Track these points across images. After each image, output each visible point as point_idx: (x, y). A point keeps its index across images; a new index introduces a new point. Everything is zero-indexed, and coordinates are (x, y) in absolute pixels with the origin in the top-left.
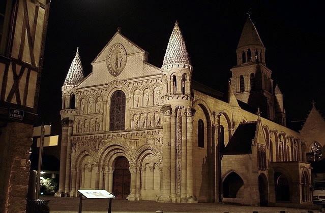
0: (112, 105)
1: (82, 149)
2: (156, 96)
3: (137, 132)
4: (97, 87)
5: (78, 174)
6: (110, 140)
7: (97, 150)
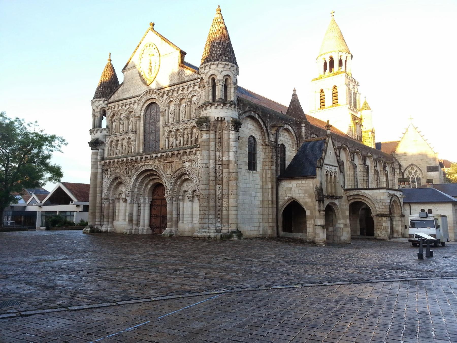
1: (114, 176)
2: (193, 106)
3: (172, 153)
4: (128, 100)
5: (111, 205)
6: (143, 164)
7: (129, 177)
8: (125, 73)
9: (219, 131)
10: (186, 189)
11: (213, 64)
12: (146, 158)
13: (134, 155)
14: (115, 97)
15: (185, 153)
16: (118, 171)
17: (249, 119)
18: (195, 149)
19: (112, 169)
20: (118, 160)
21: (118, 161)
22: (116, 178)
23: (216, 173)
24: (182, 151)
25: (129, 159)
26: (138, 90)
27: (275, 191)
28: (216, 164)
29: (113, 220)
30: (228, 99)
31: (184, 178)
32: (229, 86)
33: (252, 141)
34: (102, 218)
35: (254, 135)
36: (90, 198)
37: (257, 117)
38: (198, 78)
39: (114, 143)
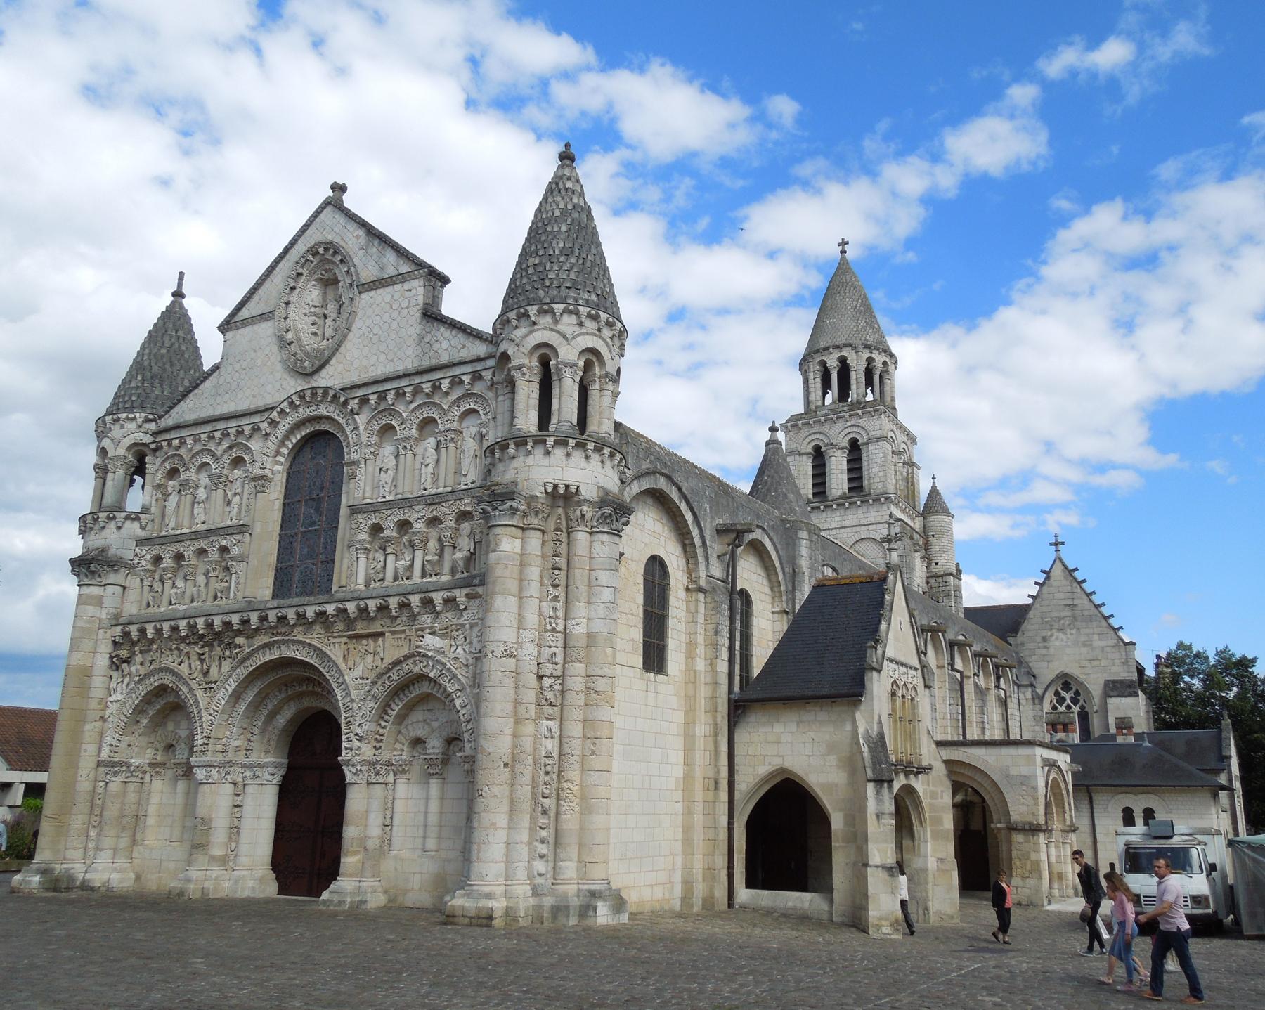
1: (155, 681)
3: (378, 601)
4: (234, 423)
8: (229, 334)
9: (558, 529)
11: (546, 312)
13: (236, 607)
14: (188, 410)
15: (427, 603)
16: (169, 661)
17: (650, 501)
18: (465, 591)
19: (149, 657)
20: (173, 623)
22: (162, 690)
23: (540, 678)
24: (417, 597)
25: (217, 621)
26: (269, 388)
27: (724, 747)
28: (540, 646)
29: (134, 842)
30: (592, 427)
31: (415, 692)
32: (597, 386)
34: (93, 833)
35: (662, 554)
36: (56, 760)
37: (675, 495)
38: (490, 356)
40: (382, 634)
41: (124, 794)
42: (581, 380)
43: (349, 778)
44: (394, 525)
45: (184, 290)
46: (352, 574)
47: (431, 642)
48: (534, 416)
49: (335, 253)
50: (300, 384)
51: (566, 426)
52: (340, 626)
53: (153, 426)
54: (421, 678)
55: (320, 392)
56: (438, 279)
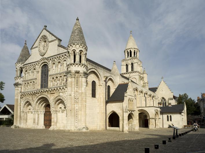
0: (42, 73)
4: (33, 63)
6: (39, 94)
7: (33, 101)
10: (61, 107)
11: (74, 45)
12: (42, 91)
14: (27, 62)
16: (28, 98)
19: (25, 97)
21: (28, 93)
22: (28, 102)
25: (33, 92)
33: (94, 83)
34: (21, 121)
38: (67, 52)
39: (27, 84)
40: (54, 93)
41: (24, 116)
42: (80, 55)
43: (52, 113)
44: (56, 77)
45: (26, 43)
46: (50, 85)
47: (61, 94)
48: (73, 61)
49: (45, 37)
50: (42, 57)
51: (78, 62)
52: (49, 92)
53: (23, 64)
54: (60, 99)
55: (44, 58)
56: (60, 40)
